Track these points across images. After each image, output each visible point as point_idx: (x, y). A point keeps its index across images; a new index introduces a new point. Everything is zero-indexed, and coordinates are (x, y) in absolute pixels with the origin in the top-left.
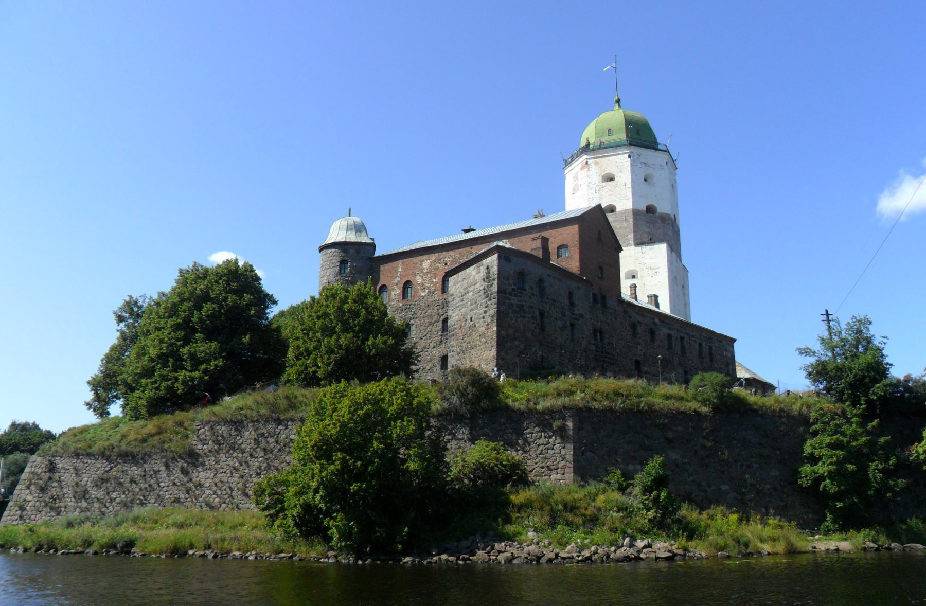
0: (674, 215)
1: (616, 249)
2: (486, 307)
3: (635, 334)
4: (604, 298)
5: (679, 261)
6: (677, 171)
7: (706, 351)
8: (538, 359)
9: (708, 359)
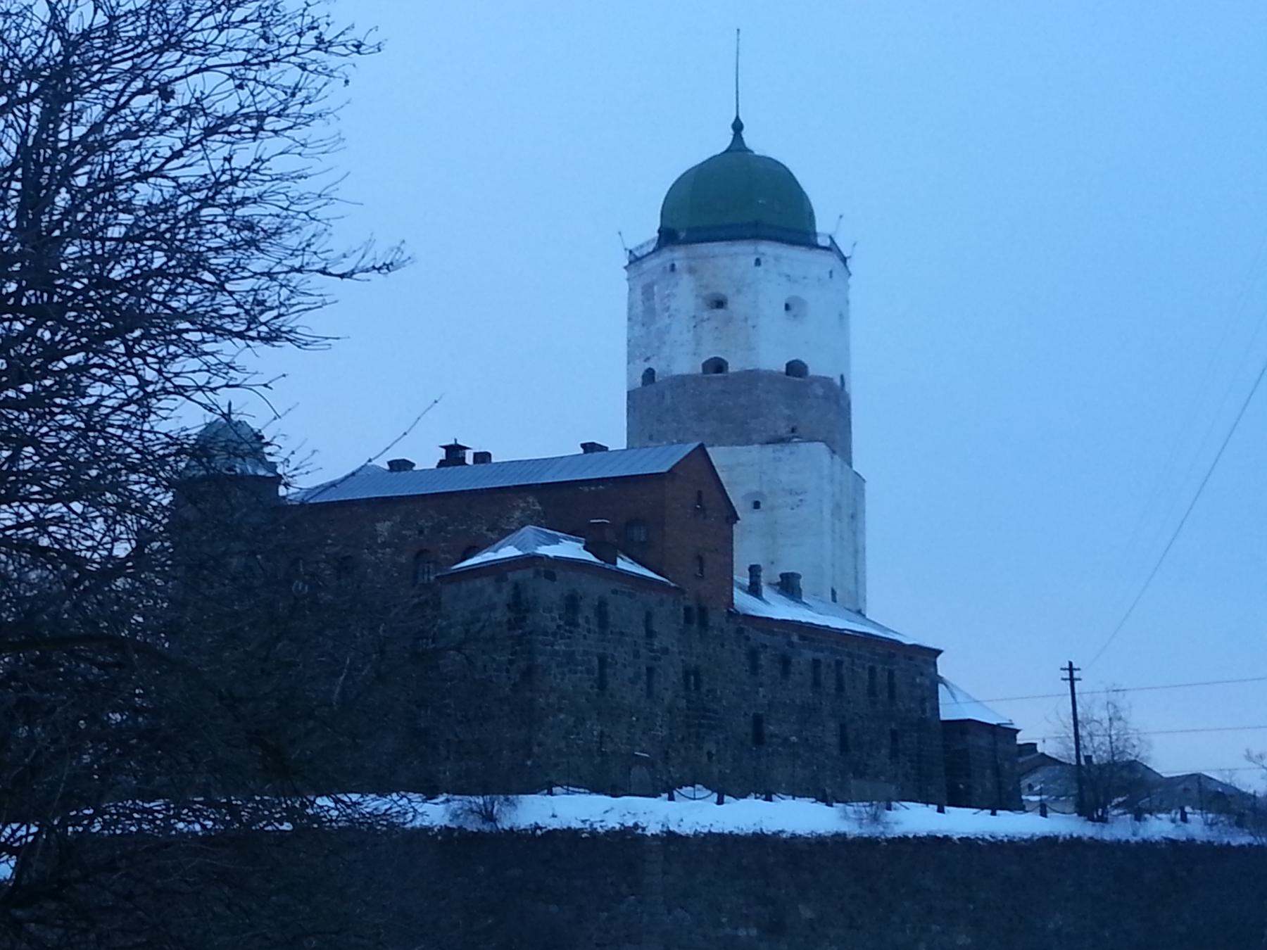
0: (842, 377)
1: (727, 519)
3: (755, 668)
4: (703, 611)
5: (847, 467)
6: (851, 281)
7: (882, 678)
8: (595, 739)
9: (883, 696)
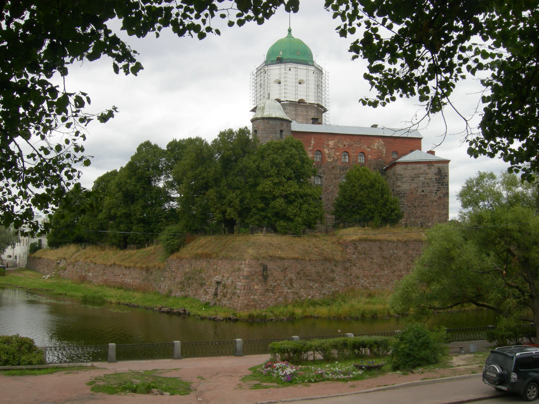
2: (438, 188)
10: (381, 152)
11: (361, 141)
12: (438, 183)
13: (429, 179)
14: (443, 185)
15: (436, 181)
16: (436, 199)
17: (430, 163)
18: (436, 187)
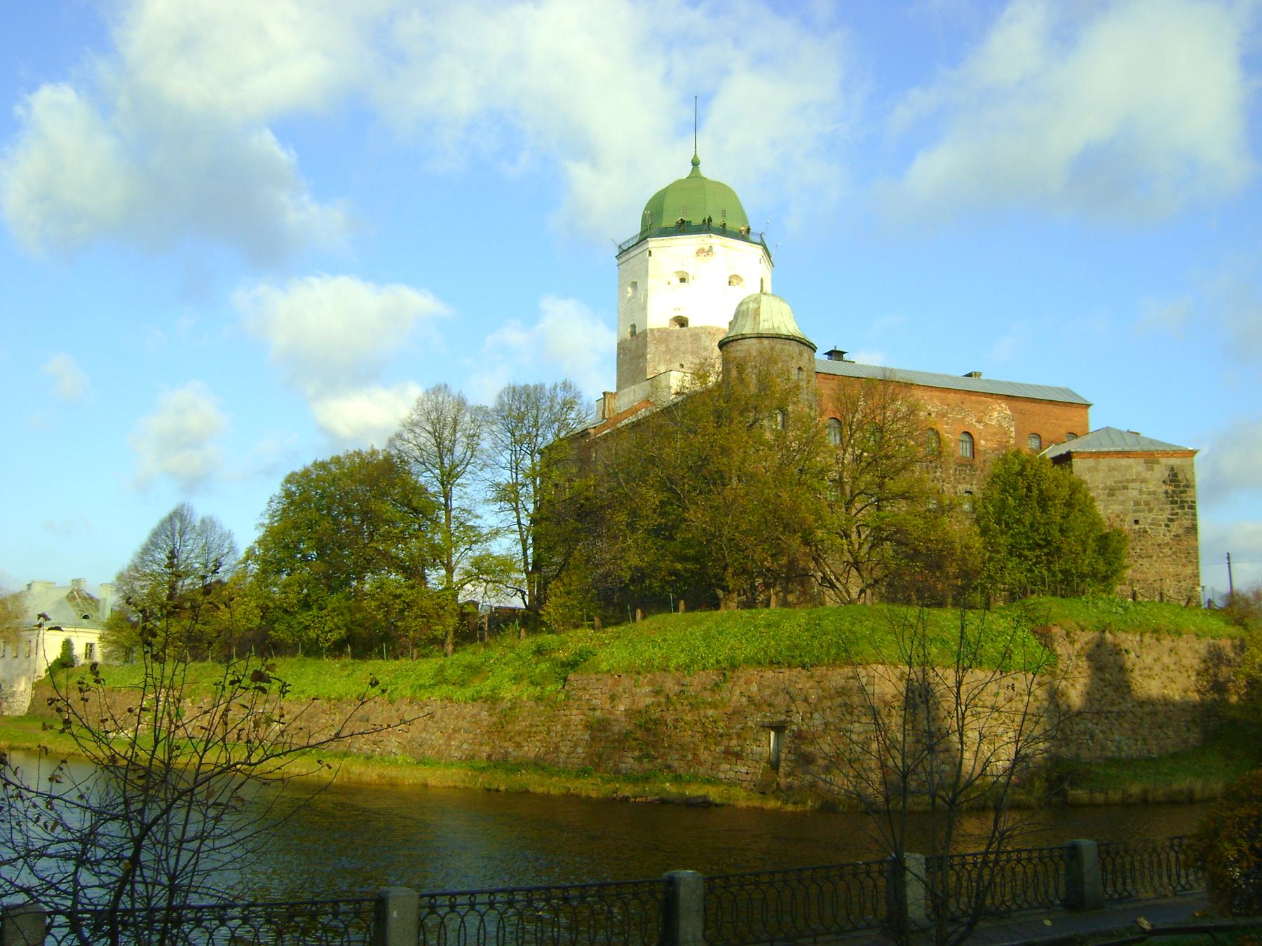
10: (1005, 433)
11: (964, 407)
12: (1172, 503)
13: (1149, 493)
14: (1182, 508)
15: (1167, 497)
16: (1167, 539)
17: (1150, 456)
18: (1168, 512)
